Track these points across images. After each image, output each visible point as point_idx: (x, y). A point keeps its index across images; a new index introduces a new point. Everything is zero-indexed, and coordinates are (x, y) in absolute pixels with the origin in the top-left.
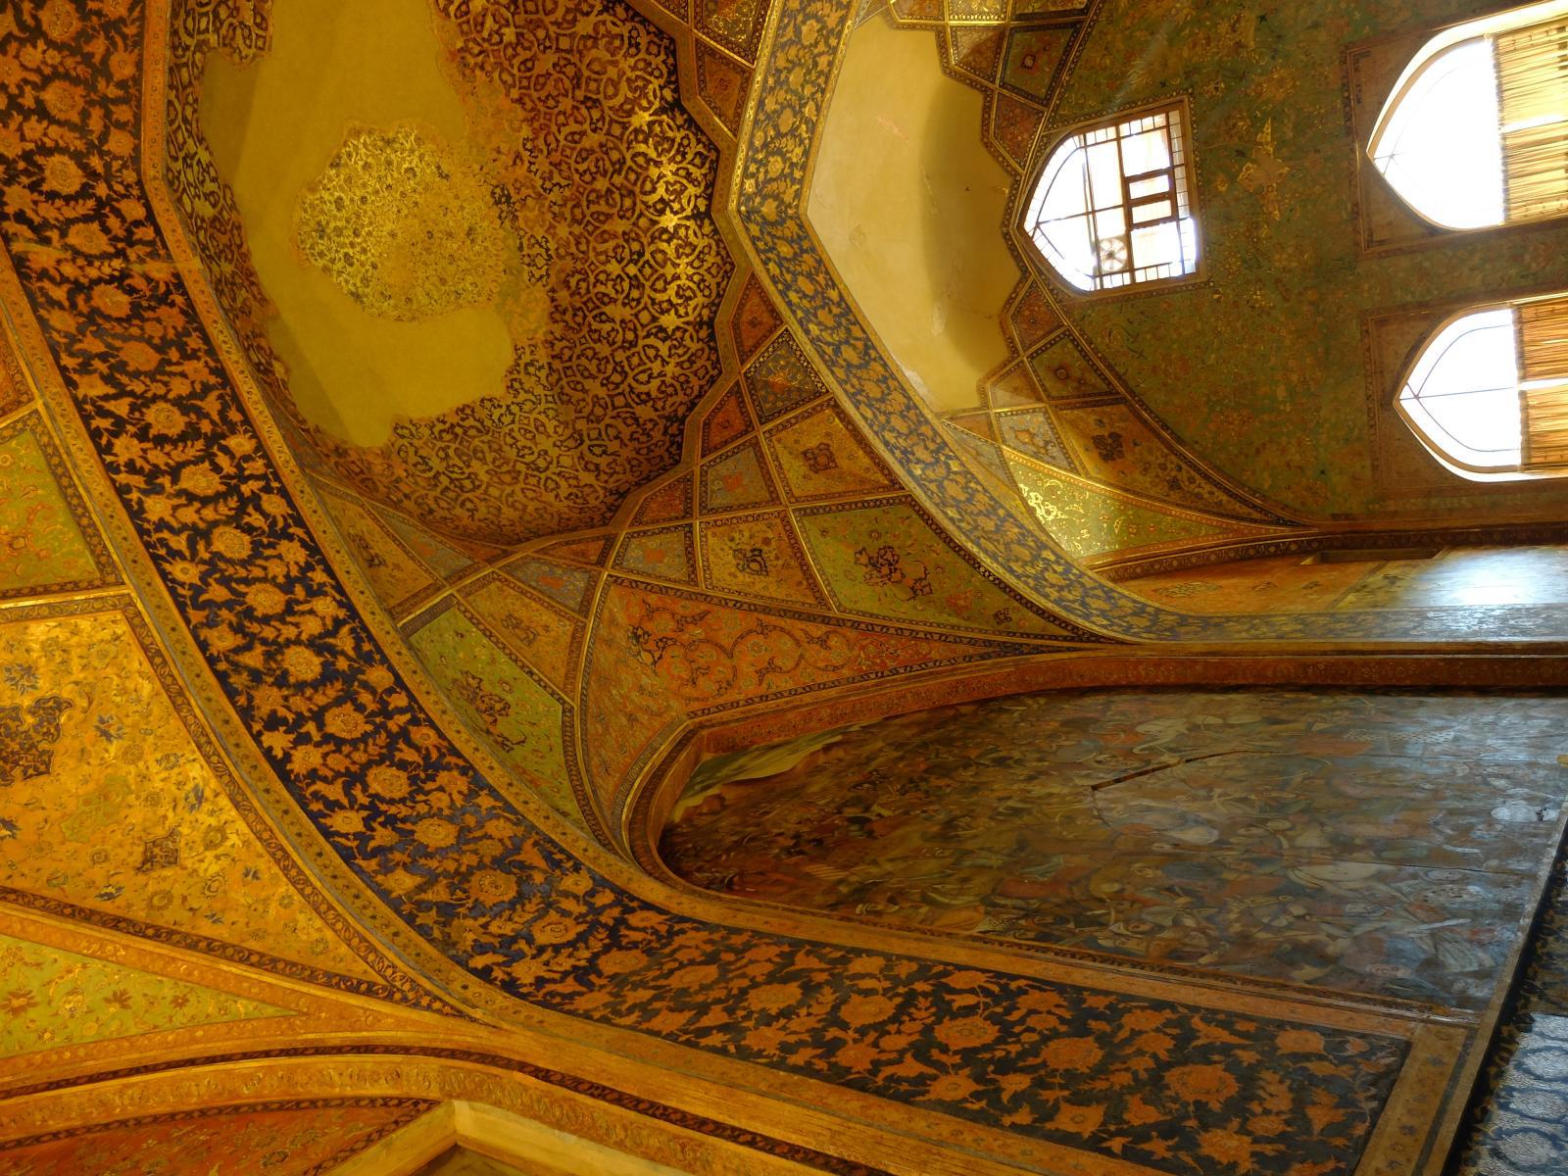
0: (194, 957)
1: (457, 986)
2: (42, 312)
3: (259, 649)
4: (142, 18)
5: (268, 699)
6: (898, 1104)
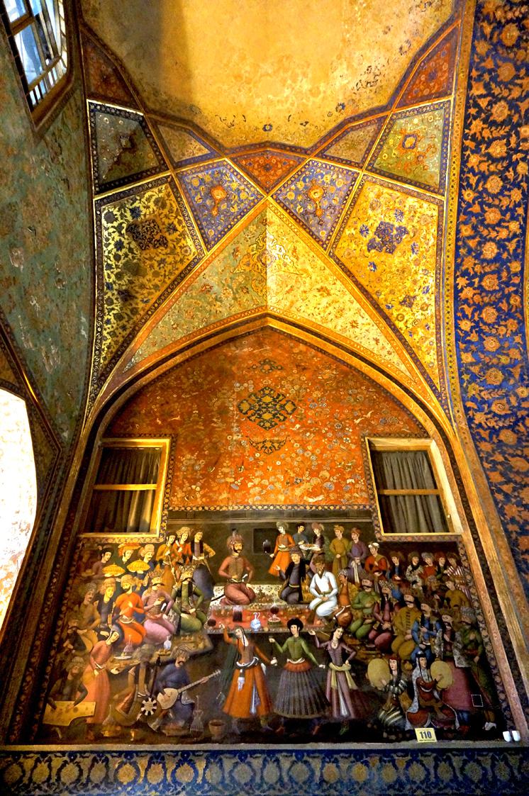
0: (400, 344)
1: (456, 409)
3: (478, 239)
5: (469, 263)
6: (516, 569)
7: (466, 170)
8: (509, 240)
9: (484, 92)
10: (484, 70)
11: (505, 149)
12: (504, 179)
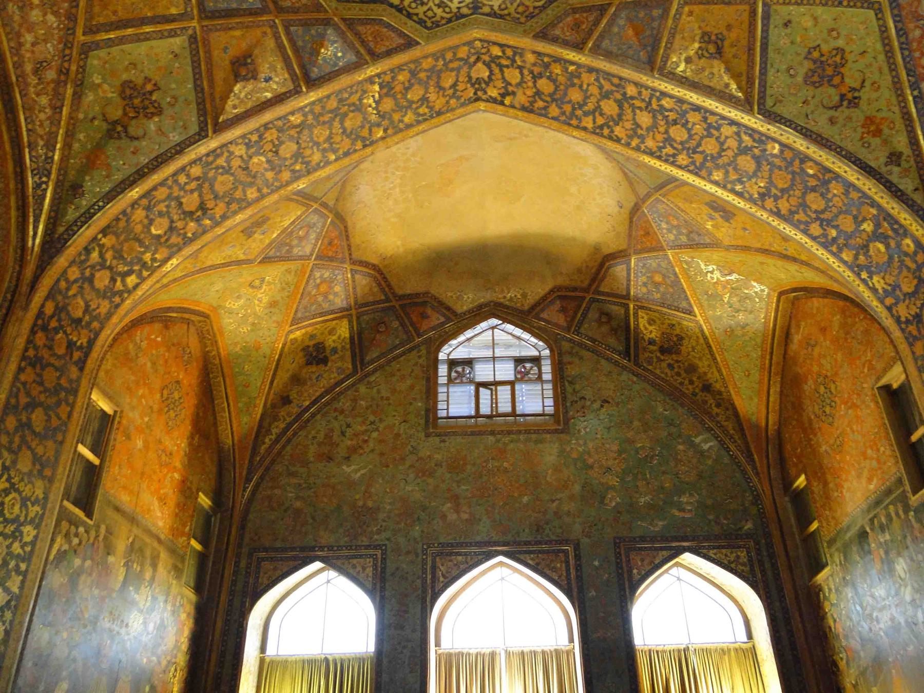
2: (550, 116)
3: (730, 169)
4: (406, 64)
7: (658, 154)
8: (740, 141)
9: (591, 117)
10: (573, 114)
11: (645, 113)
12: (675, 122)
